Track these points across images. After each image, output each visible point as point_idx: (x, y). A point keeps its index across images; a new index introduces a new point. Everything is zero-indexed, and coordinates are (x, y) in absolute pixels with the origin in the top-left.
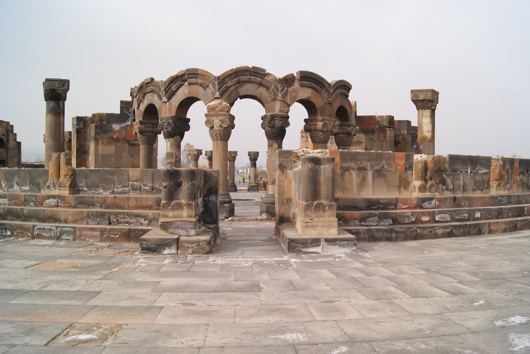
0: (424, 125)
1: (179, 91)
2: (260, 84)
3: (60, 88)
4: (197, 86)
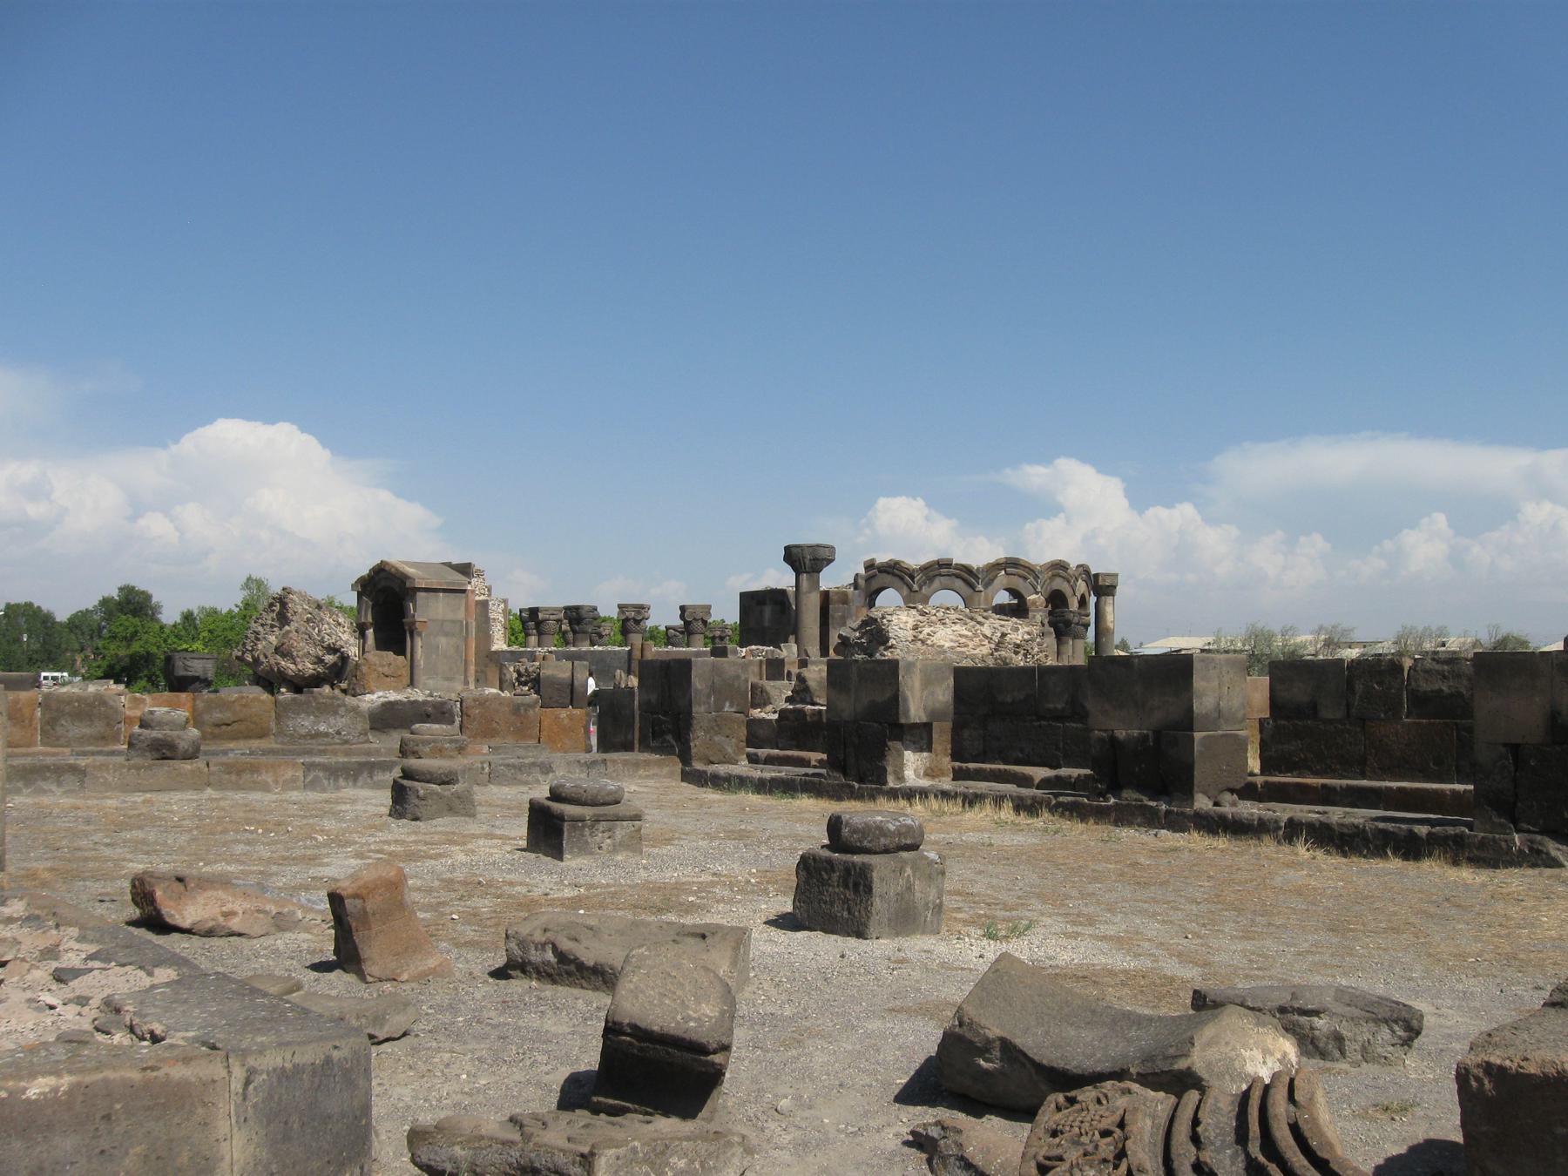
4: (1016, 577)
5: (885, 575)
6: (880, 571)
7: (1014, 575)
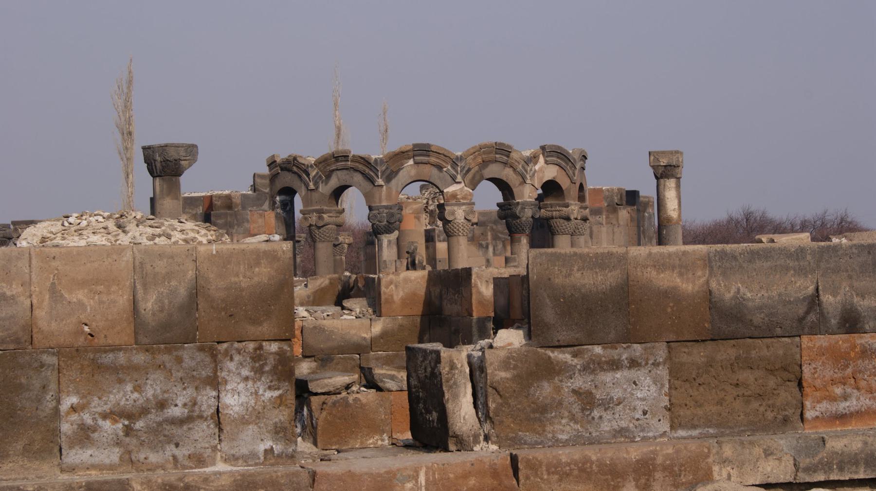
0: (667, 200)
1: (401, 171)
2: (505, 164)
3: (187, 158)
4: (429, 165)
5: (286, 173)
6: (282, 169)
7: (426, 164)
